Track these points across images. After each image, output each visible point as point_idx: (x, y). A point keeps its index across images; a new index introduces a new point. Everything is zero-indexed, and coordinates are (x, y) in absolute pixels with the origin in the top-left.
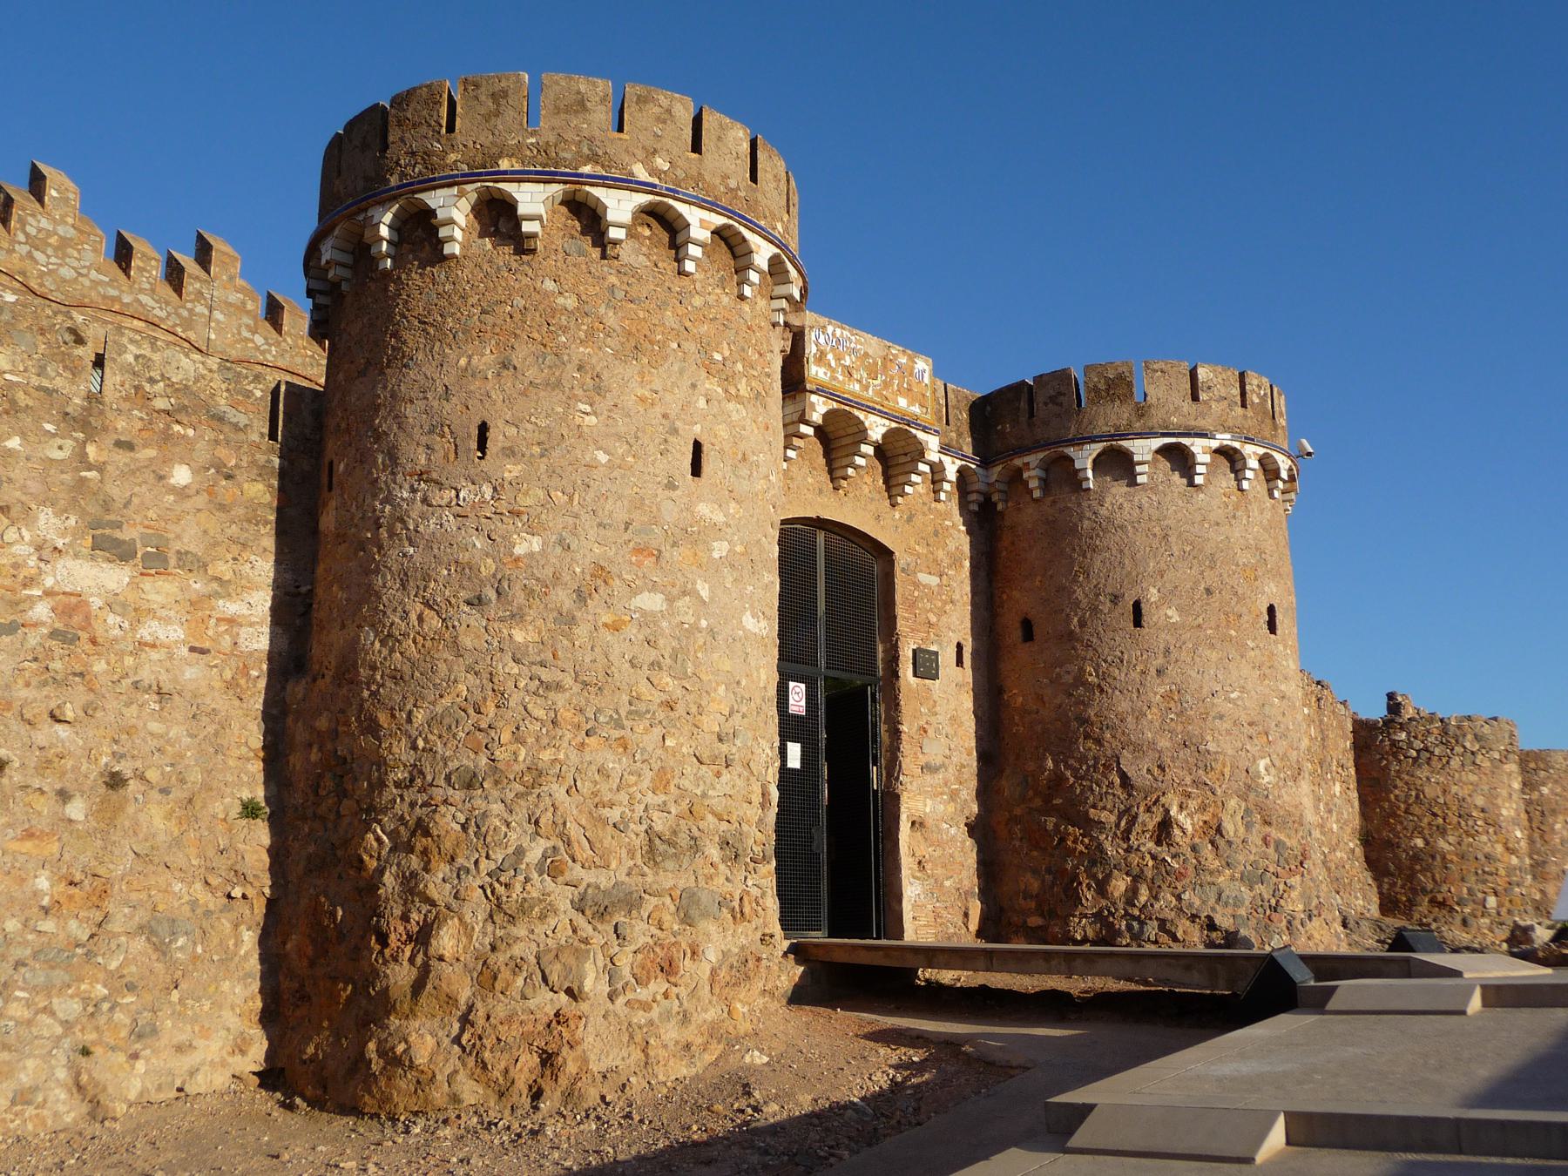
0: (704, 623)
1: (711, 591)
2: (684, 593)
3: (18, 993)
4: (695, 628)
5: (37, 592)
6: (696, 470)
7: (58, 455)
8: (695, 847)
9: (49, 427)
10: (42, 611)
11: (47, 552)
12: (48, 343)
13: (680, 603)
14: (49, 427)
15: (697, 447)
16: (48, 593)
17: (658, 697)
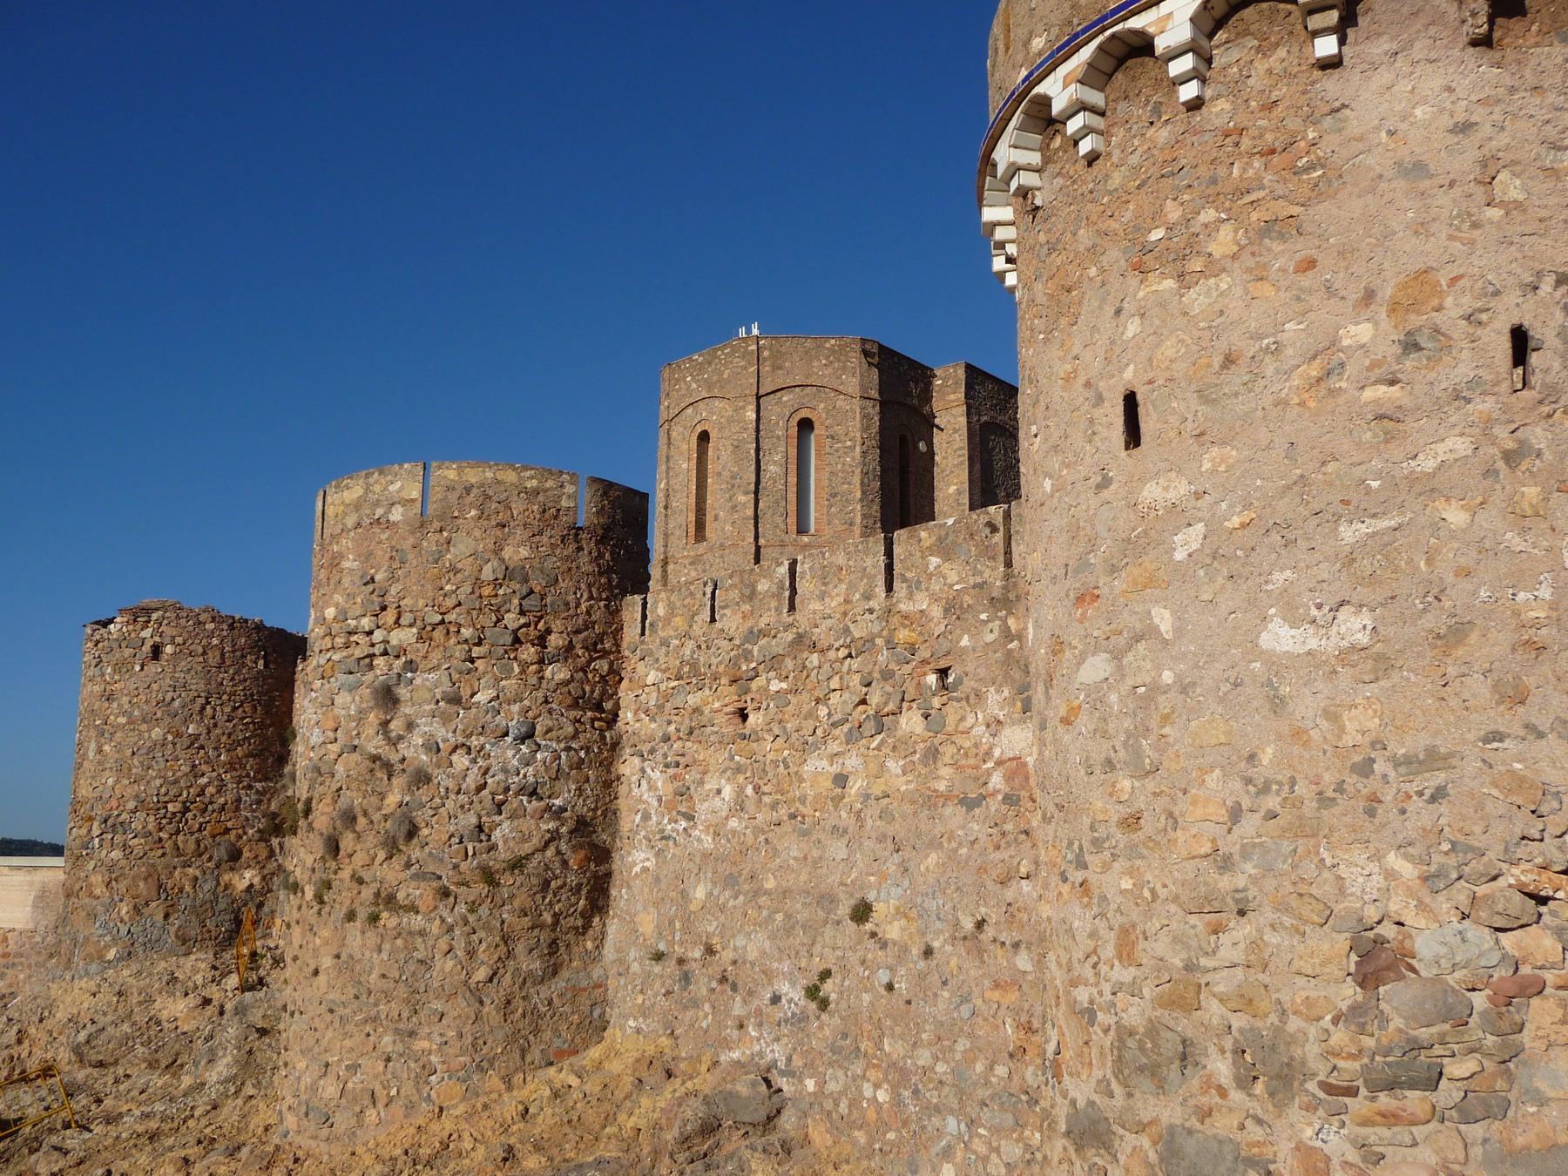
0: (1167, 677)
1: (1178, 618)
2: (1138, 638)
3: (981, 1131)
4: (1155, 688)
5: (990, 765)
6: (1133, 435)
7: (990, 638)
8: (1186, 1056)
9: (983, 616)
10: (997, 781)
11: (995, 725)
12: (976, 546)
13: (1130, 657)
14: (983, 616)
15: (1131, 402)
16: (999, 763)
17: (1115, 813)
